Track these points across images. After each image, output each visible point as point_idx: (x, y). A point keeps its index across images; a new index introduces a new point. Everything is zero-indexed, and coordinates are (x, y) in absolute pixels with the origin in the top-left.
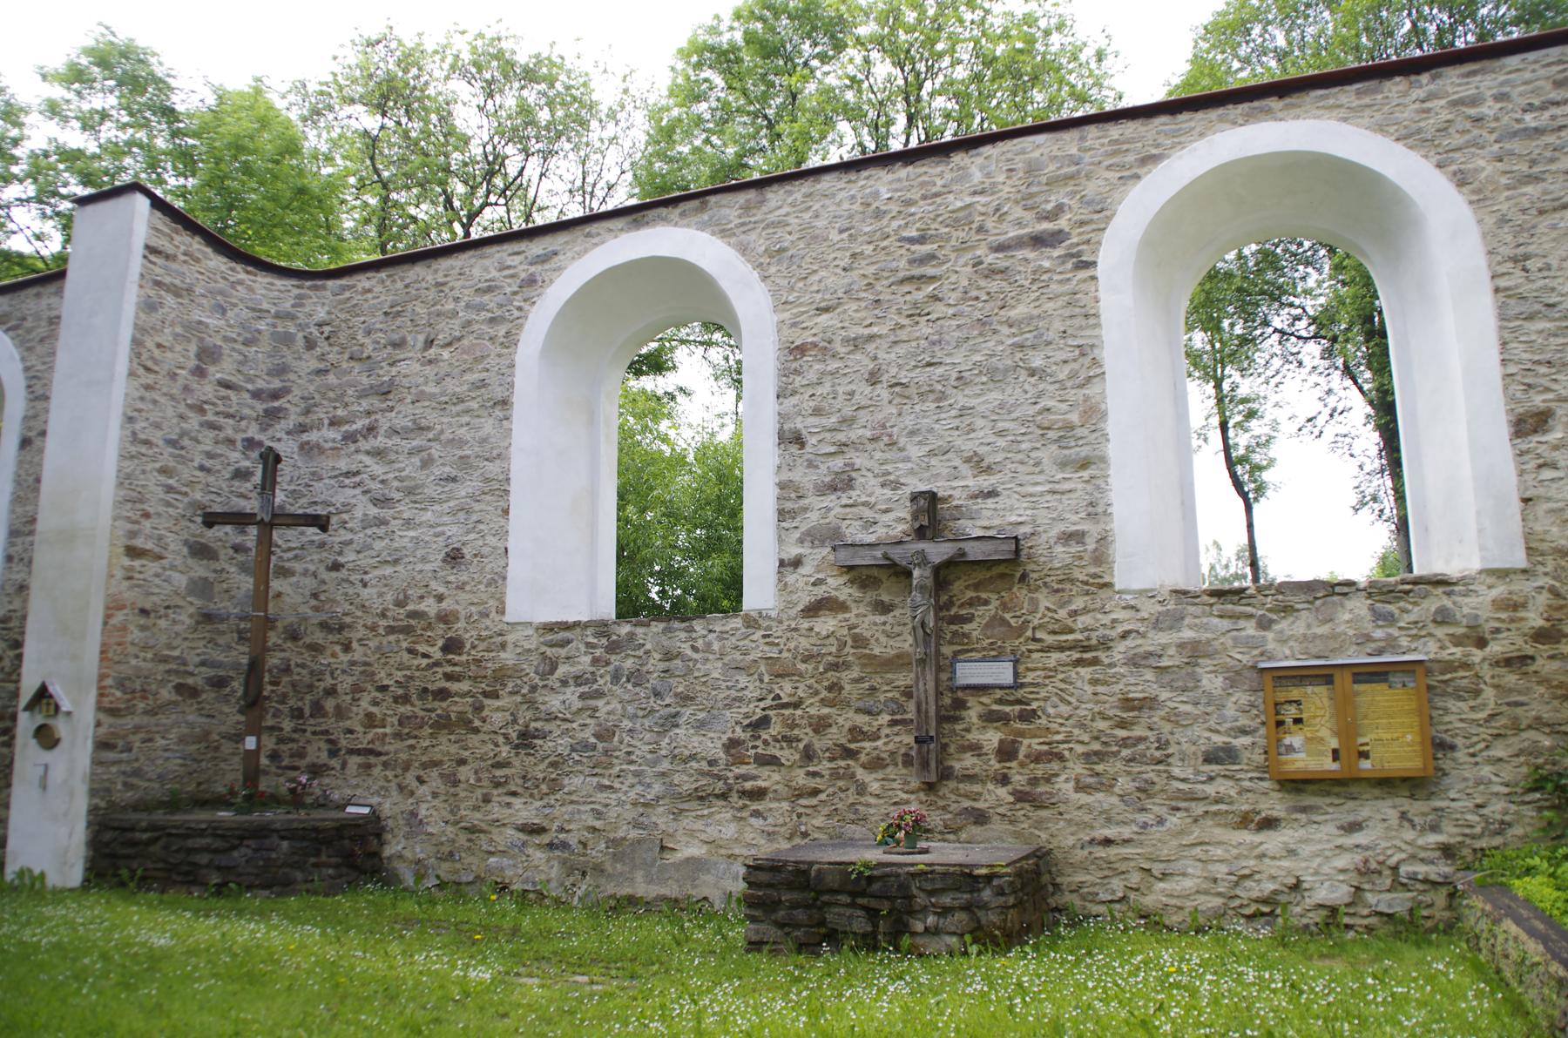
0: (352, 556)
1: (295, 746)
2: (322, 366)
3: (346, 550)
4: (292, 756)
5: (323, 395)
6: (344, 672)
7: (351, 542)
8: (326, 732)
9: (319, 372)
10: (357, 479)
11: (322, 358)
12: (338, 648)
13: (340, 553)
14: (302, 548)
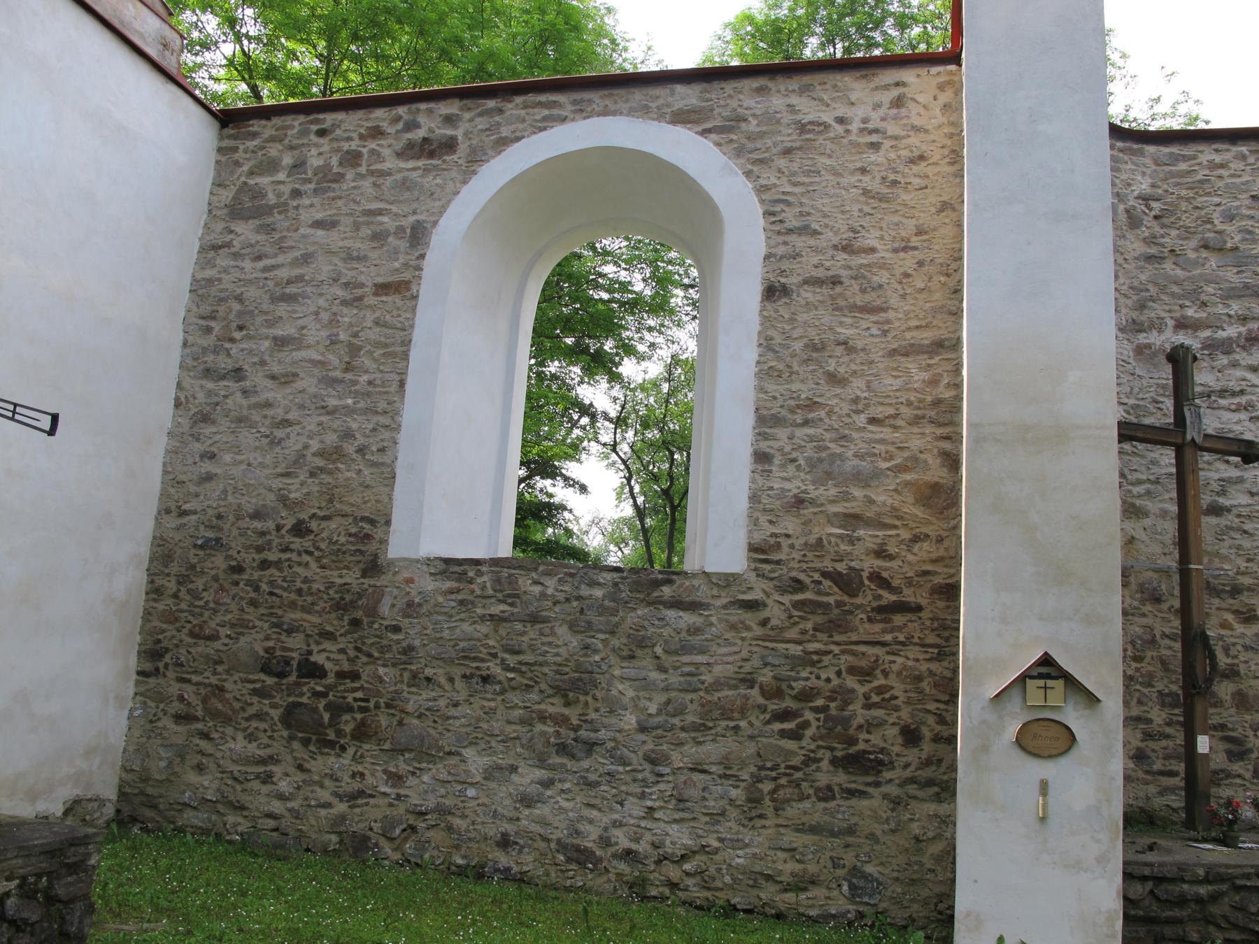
0: (1244, 499)
1: (1171, 744)
2: (1153, 250)
3: (1231, 490)
4: (1167, 757)
5: (1163, 289)
6: (1247, 648)
7: (1240, 480)
8: (1223, 727)
9: (1149, 258)
10: (1243, 400)
11: (1151, 240)
12: (1229, 617)
13: (1223, 493)
14: (1157, 482)
